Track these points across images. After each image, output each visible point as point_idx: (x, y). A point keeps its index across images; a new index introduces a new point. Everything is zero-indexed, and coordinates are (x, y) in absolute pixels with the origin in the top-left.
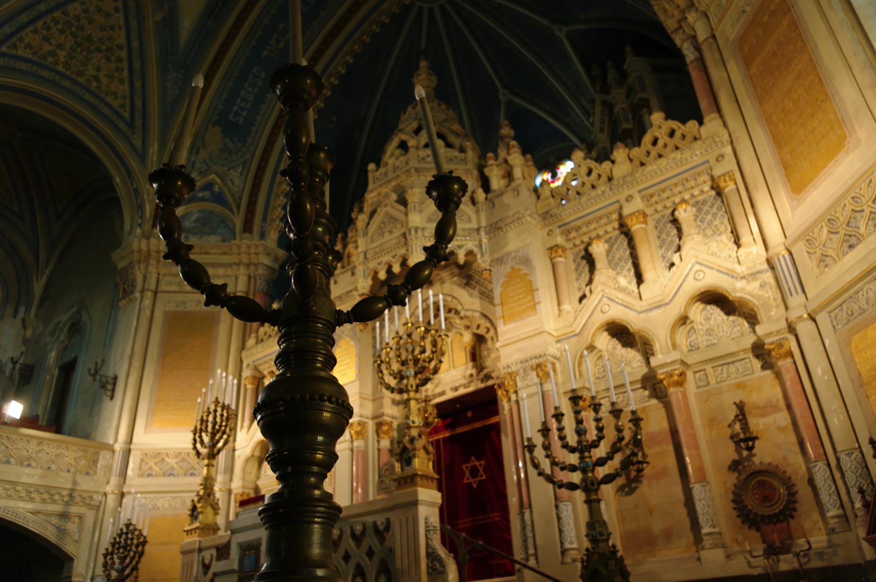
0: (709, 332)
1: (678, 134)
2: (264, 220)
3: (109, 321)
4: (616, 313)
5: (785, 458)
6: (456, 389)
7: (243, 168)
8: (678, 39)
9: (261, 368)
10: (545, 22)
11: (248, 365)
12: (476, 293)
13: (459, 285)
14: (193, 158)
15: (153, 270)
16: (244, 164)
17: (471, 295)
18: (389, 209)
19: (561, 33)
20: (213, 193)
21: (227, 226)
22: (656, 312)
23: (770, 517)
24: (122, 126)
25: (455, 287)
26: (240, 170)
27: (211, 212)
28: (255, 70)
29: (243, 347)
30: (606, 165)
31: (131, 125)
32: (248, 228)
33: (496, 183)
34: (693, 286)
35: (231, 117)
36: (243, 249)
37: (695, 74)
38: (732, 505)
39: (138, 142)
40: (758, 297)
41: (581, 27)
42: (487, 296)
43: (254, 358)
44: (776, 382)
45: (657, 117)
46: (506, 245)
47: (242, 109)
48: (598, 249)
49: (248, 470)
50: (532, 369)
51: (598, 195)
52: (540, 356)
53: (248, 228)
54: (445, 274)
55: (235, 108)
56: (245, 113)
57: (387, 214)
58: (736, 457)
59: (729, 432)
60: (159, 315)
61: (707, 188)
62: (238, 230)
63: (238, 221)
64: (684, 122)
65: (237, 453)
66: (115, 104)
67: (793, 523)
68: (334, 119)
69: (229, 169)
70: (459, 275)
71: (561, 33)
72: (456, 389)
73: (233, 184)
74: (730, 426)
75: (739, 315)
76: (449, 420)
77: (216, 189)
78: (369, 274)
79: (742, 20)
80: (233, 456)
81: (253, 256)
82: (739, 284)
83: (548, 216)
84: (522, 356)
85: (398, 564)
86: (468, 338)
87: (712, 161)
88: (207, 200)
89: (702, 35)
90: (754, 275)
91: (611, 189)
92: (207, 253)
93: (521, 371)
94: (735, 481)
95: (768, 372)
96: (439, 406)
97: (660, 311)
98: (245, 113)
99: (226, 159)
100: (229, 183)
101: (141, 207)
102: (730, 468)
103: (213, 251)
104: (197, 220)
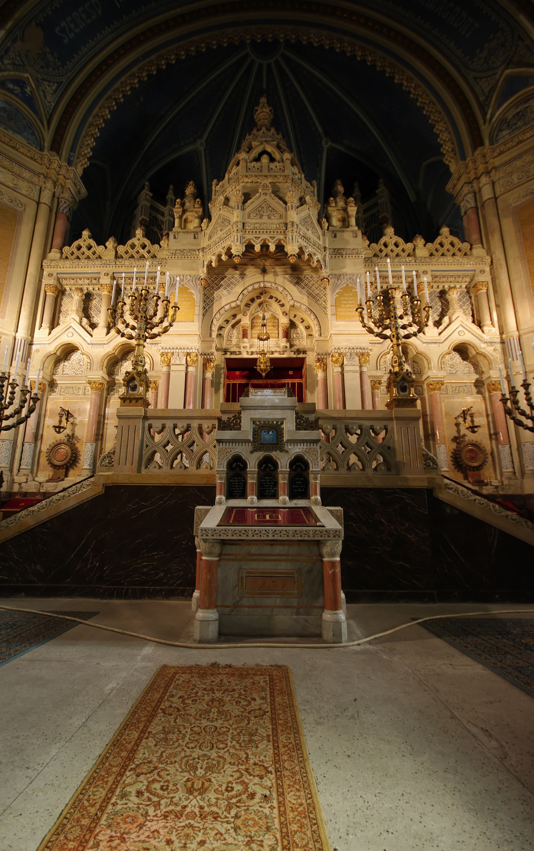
0: (452, 366)
5: (481, 440)
6: (272, 353)
7: (58, 88)
9: (64, 282)
10: (320, 130)
11: (50, 275)
12: (304, 291)
13: (291, 282)
14: (9, 44)
16: (59, 84)
17: (301, 293)
18: (268, 197)
20: (24, 93)
21: (33, 134)
22: (433, 345)
23: (474, 467)
25: (286, 281)
26: (54, 88)
29: (44, 256)
30: (410, 245)
34: (456, 339)
35: (57, 29)
36: (55, 165)
38: (451, 459)
40: (492, 355)
41: (342, 149)
43: (59, 270)
44: (483, 401)
46: (344, 267)
49: (46, 365)
50: (357, 354)
51: (406, 262)
52: (364, 348)
54: (278, 269)
55: (63, 24)
56: (72, 36)
58: (457, 435)
59: (455, 421)
61: (464, 286)
62: (47, 144)
63: (48, 136)
65: (34, 347)
67: (481, 472)
68: (142, 99)
69: (43, 80)
70: (291, 274)
72: (272, 353)
73: (45, 97)
74: (456, 418)
75: (469, 362)
76: (246, 373)
77: (28, 90)
78: (245, 242)
80: (30, 350)
81: (61, 177)
82: (483, 345)
83: (369, 261)
84: (352, 345)
85: (399, 458)
87: (478, 272)
88: (16, 95)
90: (491, 343)
91: (415, 262)
92: (14, 148)
93: (348, 354)
94: (455, 447)
95: (480, 396)
96: (272, 360)
97: (436, 345)
98: (72, 36)
99: (42, 67)
100: (41, 93)
102: (452, 440)
103: (22, 150)
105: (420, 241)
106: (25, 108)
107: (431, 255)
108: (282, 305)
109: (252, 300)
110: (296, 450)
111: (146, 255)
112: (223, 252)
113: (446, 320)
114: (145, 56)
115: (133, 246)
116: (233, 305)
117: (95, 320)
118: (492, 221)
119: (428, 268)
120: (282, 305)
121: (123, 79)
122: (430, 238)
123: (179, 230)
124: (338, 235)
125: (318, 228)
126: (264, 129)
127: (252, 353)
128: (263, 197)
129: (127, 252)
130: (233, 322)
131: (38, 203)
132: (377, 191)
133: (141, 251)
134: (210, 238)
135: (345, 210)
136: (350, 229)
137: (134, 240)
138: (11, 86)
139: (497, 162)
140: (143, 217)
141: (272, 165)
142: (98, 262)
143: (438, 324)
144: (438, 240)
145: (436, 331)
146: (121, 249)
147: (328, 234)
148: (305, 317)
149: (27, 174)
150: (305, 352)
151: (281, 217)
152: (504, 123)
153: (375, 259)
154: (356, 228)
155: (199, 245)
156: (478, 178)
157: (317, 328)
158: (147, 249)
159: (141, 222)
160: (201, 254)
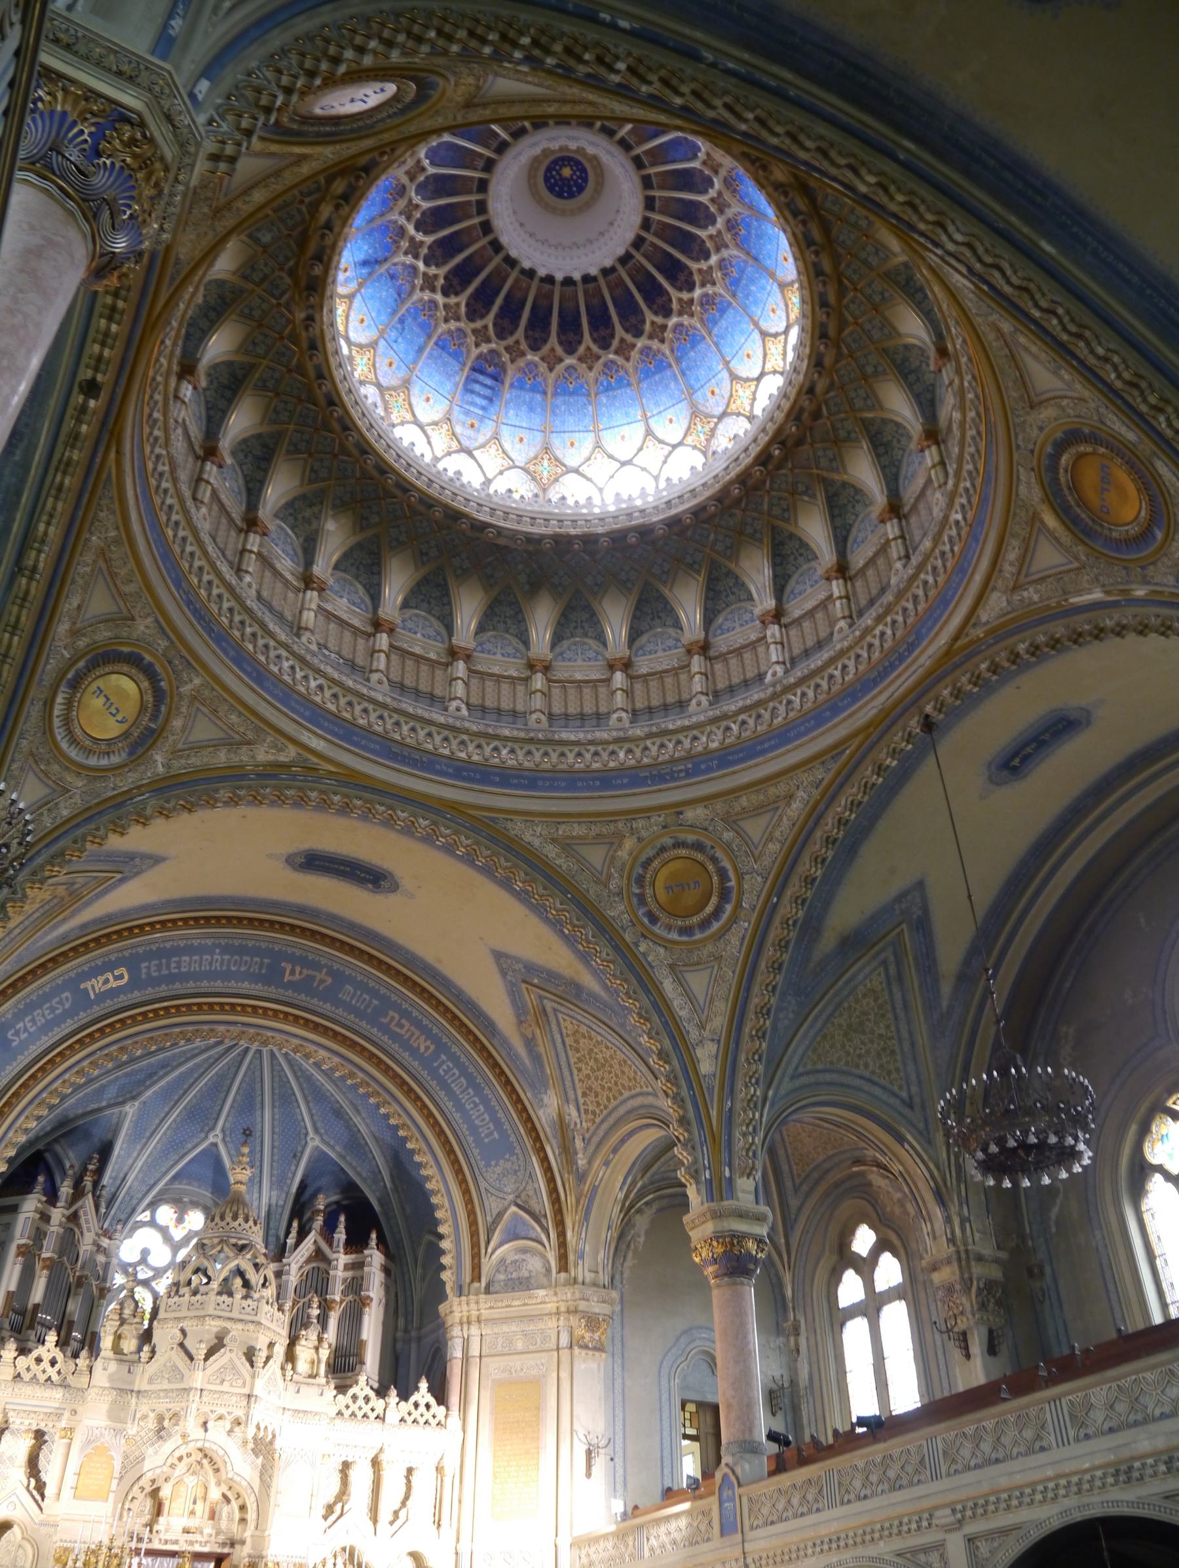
1: (432, 1411)
8: (456, 1331)
18: (233, 1355)
28: (67, 994)
30: (379, 1404)
33: (303, 1366)
41: (333, 1155)
45: (424, 1385)
47: (26, 1030)
48: (353, 1474)
55: (20, 1025)
56: (24, 1036)
57: (231, 1360)
71: (314, 1142)
79: (506, 1375)
86: (215, 1494)
89: (475, 1351)
108: (217, 1470)
109: (180, 1459)
111: (55, 1378)
112: (167, 1416)
113: (402, 1514)
114: (101, 1049)
115: (39, 1360)
116: (158, 1471)
120: (217, 1470)
121: (67, 1076)
122: (404, 1396)
123: (110, 1354)
124: (303, 1388)
126: (240, 1220)
127: (166, 1542)
129: (28, 1369)
130: (148, 1489)
132: (366, 1252)
133: (49, 1369)
134: (151, 1381)
135: (317, 1349)
137: (40, 1351)
140: (23, 1241)
141: (245, 1303)
143: (396, 1514)
146: (23, 1362)
147: (292, 1387)
148: (242, 1492)
150: (232, 1545)
151: (244, 1383)
153: (338, 1421)
154: (324, 1381)
155: (133, 1383)
157: (254, 1516)
158: (57, 1367)
159: (19, 1247)
160: (134, 1401)
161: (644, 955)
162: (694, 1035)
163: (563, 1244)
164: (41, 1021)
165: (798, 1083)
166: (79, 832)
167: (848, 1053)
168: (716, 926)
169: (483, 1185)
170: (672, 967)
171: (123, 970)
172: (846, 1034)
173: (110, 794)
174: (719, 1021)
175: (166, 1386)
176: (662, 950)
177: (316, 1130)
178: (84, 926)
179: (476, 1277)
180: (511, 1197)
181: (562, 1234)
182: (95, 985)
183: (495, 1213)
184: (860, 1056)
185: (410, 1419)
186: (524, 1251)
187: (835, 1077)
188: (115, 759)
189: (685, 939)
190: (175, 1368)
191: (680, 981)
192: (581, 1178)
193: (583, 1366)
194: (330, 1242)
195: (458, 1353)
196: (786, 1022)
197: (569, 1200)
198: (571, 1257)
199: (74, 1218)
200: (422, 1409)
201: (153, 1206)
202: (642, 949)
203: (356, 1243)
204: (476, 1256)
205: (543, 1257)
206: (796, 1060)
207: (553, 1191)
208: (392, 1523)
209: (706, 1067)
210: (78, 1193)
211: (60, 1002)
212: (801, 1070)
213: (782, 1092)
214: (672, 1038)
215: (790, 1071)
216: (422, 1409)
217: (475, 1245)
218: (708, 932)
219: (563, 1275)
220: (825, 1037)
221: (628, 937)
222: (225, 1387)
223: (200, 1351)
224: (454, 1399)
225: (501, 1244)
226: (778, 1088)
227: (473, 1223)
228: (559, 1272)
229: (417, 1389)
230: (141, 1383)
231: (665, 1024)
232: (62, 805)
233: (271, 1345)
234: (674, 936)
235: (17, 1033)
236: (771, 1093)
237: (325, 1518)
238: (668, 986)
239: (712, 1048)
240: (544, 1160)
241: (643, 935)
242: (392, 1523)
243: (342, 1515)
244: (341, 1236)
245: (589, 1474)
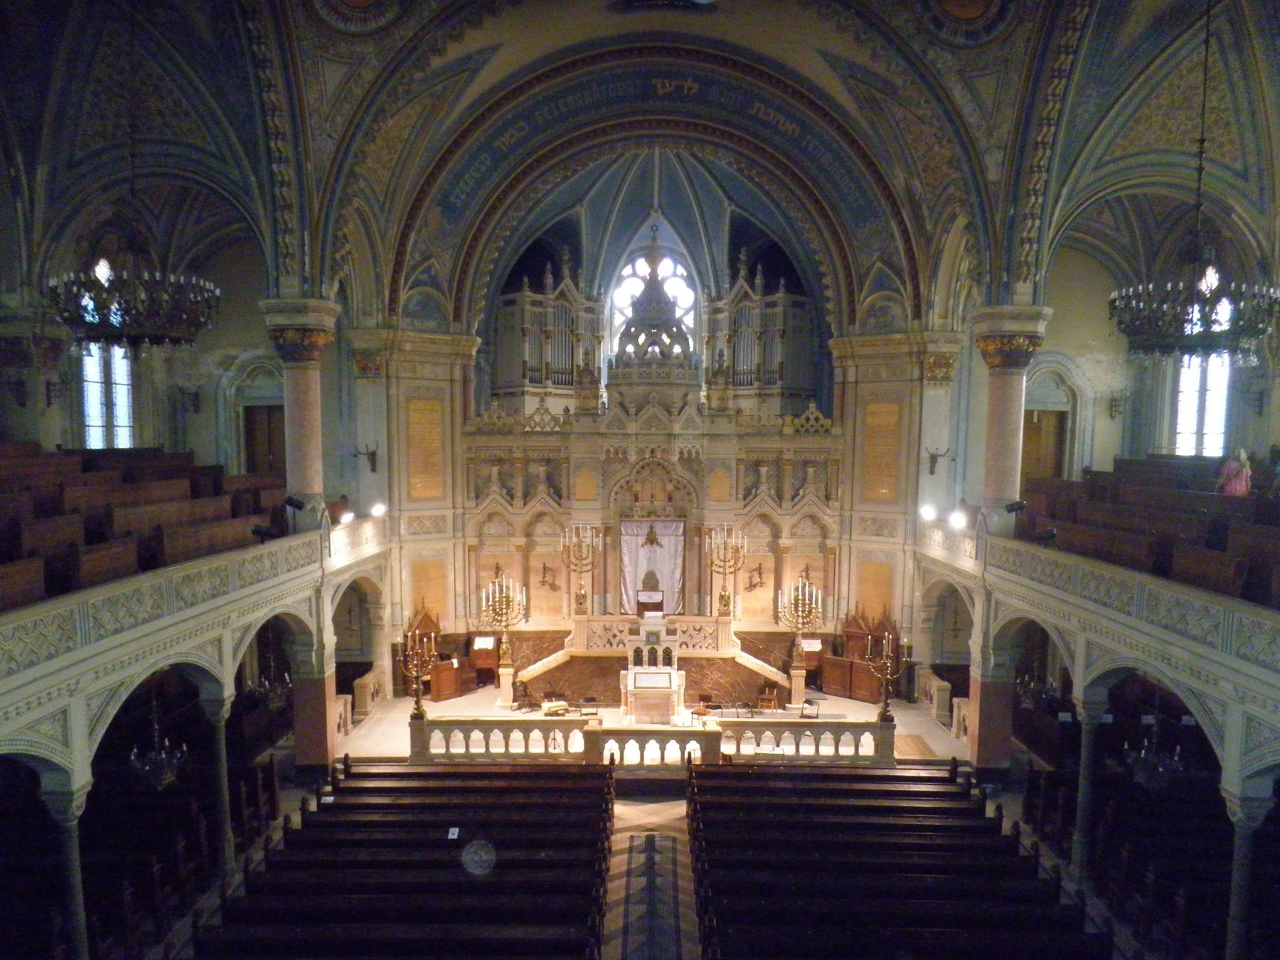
2: (469, 310)
3: (340, 391)
4: (767, 510)
8: (836, 363)
15: (395, 357)
19: (728, 208)
24: (377, 210)
27: (428, 296)
31: (382, 208)
32: (457, 317)
34: (806, 510)
35: (452, 199)
37: (837, 391)
39: (382, 225)
42: (696, 473)
45: (812, 406)
53: (457, 317)
55: (457, 191)
60: (402, 398)
63: (451, 307)
64: (826, 417)
66: (378, 190)
86: (670, 487)
89: (851, 377)
101: (380, 292)
104: (419, 303)
105: (788, 419)
106: (434, 292)
107: (797, 431)
110: (664, 645)
113: (801, 492)
117: (509, 484)
118: (849, 408)
119: (792, 446)
125: (698, 420)
128: (652, 410)
131: (452, 381)
136: (727, 413)
138: (421, 277)
139: (860, 351)
141: (660, 371)
142: (510, 438)
144: (804, 416)
145: (790, 504)
149: (442, 360)
152: (872, 311)
156: (846, 357)
161: (934, 62)
162: (982, 142)
163: (917, 295)
164: (472, 182)
165: (1102, 172)
166: (389, 86)
167: (1170, 131)
168: (1001, 26)
169: (855, 244)
170: (961, 73)
171: (522, 123)
172: (1166, 115)
173: (400, 45)
174: (1005, 128)
175: (616, 431)
176: (948, 56)
177: (730, 199)
178: (472, 107)
179: (852, 320)
180: (877, 254)
181: (916, 287)
182: (504, 141)
183: (866, 266)
184: (1184, 132)
185: (803, 430)
186: (889, 299)
187: (1153, 158)
188: (390, 16)
189: (971, 43)
190: (620, 420)
191: (969, 87)
192: (929, 241)
193: (932, 392)
194: (752, 286)
195: (838, 378)
196: (1086, 116)
197: (920, 258)
198: (924, 308)
199: (562, 294)
200: (812, 422)
201: (632, 261)
202: (930, 57)
203: (769, 288)
204: (852, 303)
205: (903, 304)
206: (1100, 151)
207: (909, 250)
208: (793, 499)
209: (993, 175)
210: (558, 278)
211: (482, 163)
212: (1107, 158)
213: (1082, 184)
214: (963, 146)
215: (1093, 162)
216: (812, 422)
217: (851, 294)
218: (994, 34)
219: (916, 322)
220: (1138, 121)
221: (917, 47)
222: (653, 430)
223: (632, 411)
224: (836, 413)
225: (871, 292)
226: (1077, 182)
227: (849, 275)
228: (913, 319)
229: (808, 408)
230: (603, 430)
231: (957, 132)
232: (363, 73)
233: (686, 395)
234: (960, 40)
235: (457, 197)
236: (1065, 191)
237: (745, 498)
238: (959, 94)
239: (999, 156)
240: (901, 223)
241: (931, 43)
242: (793, 499)
243: (756, 496)
244: (759, 281)
245: (932, 472)
